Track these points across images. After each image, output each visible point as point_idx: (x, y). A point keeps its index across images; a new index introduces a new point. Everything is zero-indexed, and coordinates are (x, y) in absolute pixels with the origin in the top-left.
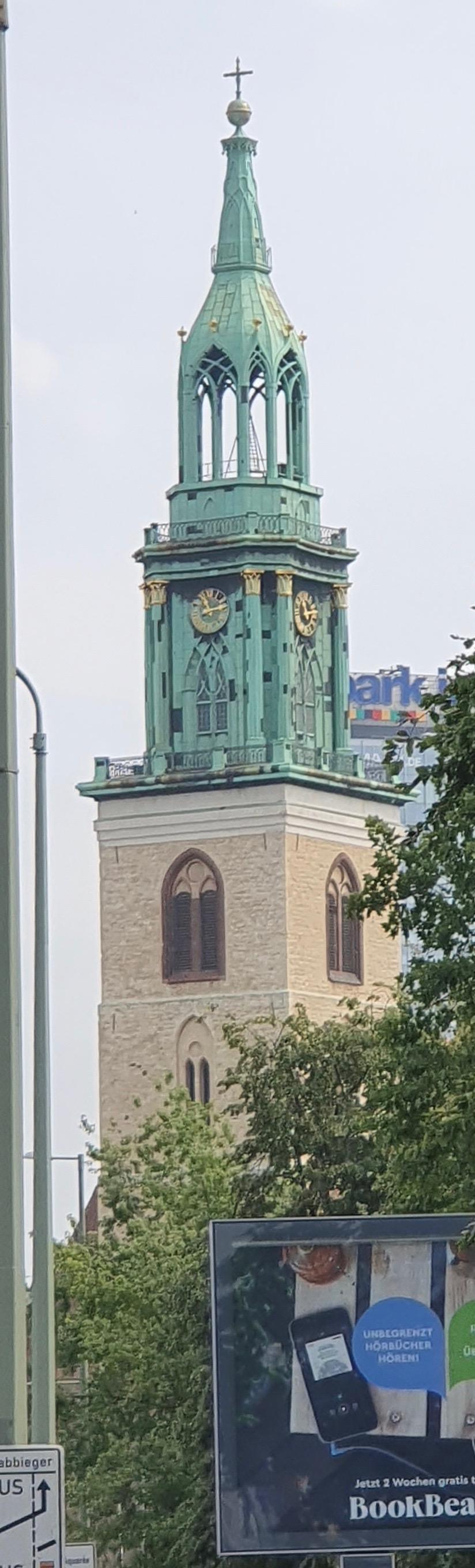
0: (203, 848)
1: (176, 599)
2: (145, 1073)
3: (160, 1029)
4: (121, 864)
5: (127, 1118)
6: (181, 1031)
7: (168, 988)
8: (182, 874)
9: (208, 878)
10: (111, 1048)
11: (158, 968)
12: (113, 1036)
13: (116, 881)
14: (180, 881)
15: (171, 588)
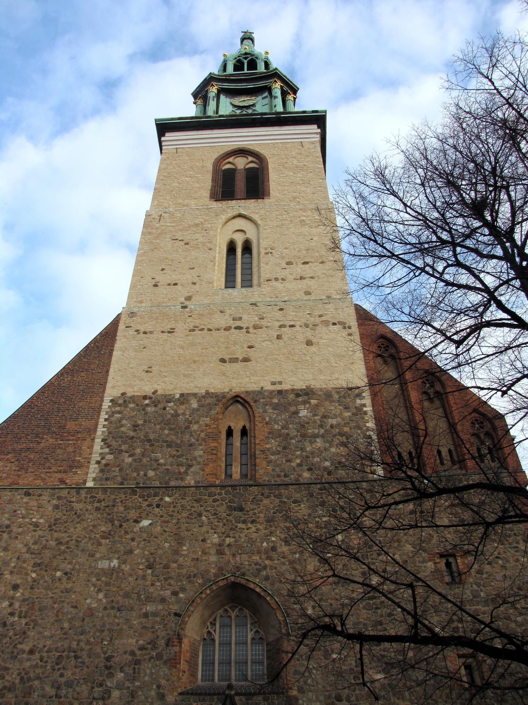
0: (251, 147)
1: (222, 97)
2: (187, 244)
3: (205, 220)
4: (178, 154)
5: (163, 269)
6: (226, 223)
7: (215, 203)
8: (231, 160)
9: (252, 162)
10: (154, 231)
11: (207, 194)
12: (157, 225)
13: (175, 160)
14: (229, 163)
15: (220, 91)
